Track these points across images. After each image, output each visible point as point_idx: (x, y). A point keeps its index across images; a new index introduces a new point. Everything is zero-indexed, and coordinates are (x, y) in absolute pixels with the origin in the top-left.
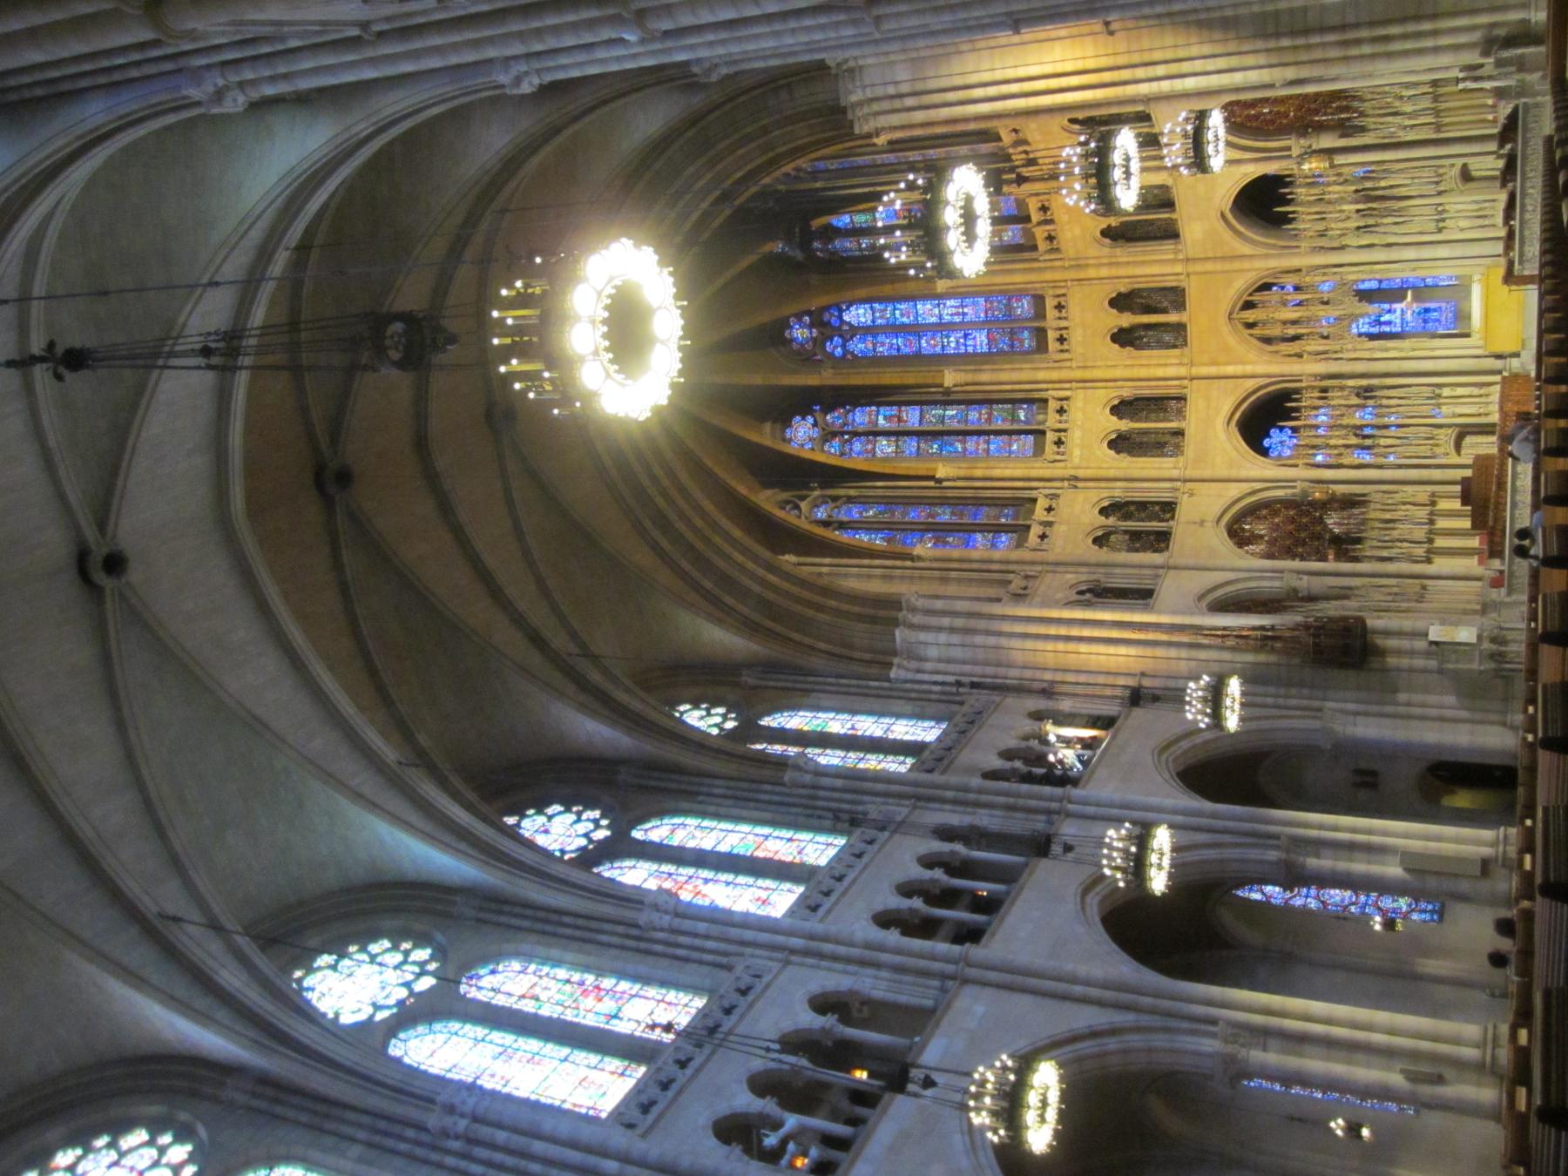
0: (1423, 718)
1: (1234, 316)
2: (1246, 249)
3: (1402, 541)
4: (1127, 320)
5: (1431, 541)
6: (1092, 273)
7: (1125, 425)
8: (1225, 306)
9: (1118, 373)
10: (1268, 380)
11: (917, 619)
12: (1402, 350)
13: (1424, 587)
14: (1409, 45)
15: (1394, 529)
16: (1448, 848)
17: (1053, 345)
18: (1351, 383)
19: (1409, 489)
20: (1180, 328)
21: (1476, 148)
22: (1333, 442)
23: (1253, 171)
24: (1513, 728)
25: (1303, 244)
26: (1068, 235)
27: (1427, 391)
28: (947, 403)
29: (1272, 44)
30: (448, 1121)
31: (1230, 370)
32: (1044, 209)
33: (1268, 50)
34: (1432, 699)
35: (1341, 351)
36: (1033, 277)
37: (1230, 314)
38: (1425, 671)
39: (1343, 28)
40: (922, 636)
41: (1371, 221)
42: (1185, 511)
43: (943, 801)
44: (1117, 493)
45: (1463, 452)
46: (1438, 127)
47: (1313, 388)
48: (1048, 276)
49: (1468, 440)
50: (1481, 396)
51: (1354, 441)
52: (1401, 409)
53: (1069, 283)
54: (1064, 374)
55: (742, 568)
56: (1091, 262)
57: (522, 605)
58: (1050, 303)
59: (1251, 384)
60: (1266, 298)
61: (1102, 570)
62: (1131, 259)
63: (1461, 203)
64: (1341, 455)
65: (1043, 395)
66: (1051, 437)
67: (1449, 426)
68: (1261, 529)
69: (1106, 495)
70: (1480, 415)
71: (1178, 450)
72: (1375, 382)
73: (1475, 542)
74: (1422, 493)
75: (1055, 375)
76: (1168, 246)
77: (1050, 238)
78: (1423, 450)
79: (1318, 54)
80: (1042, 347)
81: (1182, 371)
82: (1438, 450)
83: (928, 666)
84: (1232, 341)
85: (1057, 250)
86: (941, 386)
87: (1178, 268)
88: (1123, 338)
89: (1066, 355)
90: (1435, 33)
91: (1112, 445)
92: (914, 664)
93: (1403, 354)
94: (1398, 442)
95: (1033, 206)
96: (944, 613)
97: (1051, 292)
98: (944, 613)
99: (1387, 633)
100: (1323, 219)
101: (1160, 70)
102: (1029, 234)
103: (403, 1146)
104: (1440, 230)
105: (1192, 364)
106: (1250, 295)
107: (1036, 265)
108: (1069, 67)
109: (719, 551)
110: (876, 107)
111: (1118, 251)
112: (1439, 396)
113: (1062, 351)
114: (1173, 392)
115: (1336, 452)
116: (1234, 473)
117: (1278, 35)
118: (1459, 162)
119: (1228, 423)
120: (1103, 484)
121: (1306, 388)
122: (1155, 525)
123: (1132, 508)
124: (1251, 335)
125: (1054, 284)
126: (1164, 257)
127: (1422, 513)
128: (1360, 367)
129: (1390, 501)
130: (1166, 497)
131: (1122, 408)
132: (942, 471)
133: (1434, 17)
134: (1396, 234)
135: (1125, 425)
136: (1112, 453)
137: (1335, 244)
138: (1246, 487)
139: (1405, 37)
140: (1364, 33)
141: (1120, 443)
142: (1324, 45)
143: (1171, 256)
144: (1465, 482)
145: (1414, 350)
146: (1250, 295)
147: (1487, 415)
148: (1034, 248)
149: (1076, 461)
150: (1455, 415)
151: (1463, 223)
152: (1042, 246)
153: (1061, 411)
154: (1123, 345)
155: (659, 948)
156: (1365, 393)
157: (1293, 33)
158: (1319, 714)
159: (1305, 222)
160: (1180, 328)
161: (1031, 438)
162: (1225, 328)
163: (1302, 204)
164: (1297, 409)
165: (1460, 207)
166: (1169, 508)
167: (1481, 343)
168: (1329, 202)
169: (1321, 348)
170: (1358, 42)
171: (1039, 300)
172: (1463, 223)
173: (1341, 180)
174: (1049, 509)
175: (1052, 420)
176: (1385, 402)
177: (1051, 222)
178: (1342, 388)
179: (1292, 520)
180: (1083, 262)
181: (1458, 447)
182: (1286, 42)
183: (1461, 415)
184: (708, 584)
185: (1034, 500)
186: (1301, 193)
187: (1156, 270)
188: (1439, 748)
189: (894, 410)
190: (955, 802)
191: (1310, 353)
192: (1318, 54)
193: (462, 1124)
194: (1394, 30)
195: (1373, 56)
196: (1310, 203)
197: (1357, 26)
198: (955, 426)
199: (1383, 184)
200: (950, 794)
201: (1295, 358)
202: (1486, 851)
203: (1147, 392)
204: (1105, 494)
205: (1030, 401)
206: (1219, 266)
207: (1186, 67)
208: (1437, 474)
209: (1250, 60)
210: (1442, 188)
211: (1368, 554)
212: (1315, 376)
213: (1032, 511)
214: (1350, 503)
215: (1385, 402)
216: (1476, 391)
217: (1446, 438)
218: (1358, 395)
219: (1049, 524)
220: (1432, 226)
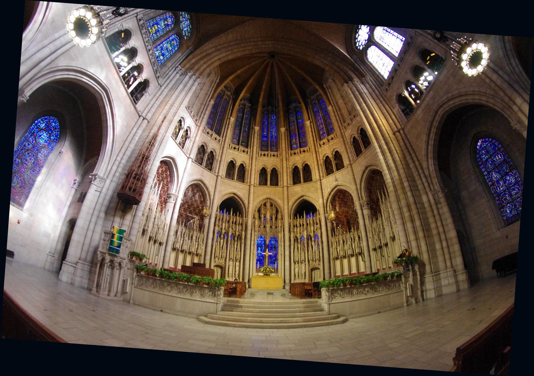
1: (268, 200)
2: (291, 204)
3: (183, 241)
5: (182, 251)
6: (285, 162)
8: (272, 197)
10: (247, 208)
12: (253, 250)
13: (160, 244)
15: (189, 239)
18: (243, 233)
19: (204, 248)
20: (266, 184)
21: (327, 271)
22: (224, 224)
23: (319, 203)
25: (292, 220)
26: (296, 157)
27: (238, 257)
29: (404, 179)
31: (252, 196)
33: (401, 180)
35: (255, 231)
36: (284, 149)
37: (270, 199)
41: (299, 241)
44: (217, 157)
45: (215, 268)
47: (243, 222)
48: (284, 152)
49: (219, 270)
50: (235, 275)
51: (223, 231)
52: (233, 248)
53: (281, 157)
56: (288, 163)
59: (246, 202)
60: (274, 209)
61: (193, 139)
62: (288, 173)
63: (304, 268)
64: (219, 227)
65: (249, 147)
67: (225, 263)
69: (217, 154)
70: (228, 274)
72: (243, 241)
76: (292, 183)
78: (217, 254)
79: (402, 196)
81: (252, 183)
82: (217, 259)
84: (261, 198)
85: (291, 155)
86: (255, 126)
87: (285, 184)
88: (263, 171)
89: (260, 155)
90: (417, 239)
91: (232, 162)
93: (252, 250)
94: (221, 246)
95: (305, 149)
97: (279, 153)
100: (300, 226)
101: (385, 147)
104: (295, 263)
105: (254, 186)
106: (275, 205)
107: (287, 150)
111: (291, 169)
112: (236, 261)
113: (261, 155)
115: (220, 225)
116: (217, 191)
118: (321, 267)
119: (234, 194)
120: (220, 154)
121: (243, 219)
123: (211, 161)
124: (262, 205)
125: (281, 154)
126: (289, 181)
127: (193, 250)
128: (249, 236)
129: (200, 240)
134: (294, 248)
136: (229, 161)
137: (292, 230)
138: (212, 193)
139: (414, 228)
140: (414, 212)
142: (406, 198)
143: (289, 183)
144: (204, 265)
145: (253, 254)
146: (275, 205)
147: (228, 276)
149: (229, 150)
150: (229, 266)
151: (297, 270)
152: (293, 152)
154: (261, 170)
156: (240, 237)
158: (105, 177)
159: (299, 221)
160: (266, 184)
162: (265, 197)
163: (306, 219)
164: (236, 215)
165: (303, 268)
167: (254, 276)
168: (307, 227)
169: (256, 225)
170: (410, 210)
172: (297, 270)
173: (315, 230)
174: (216, 139)
175: (242, 148)
176: (236, 243)
177: (301, 153)
178: (242, 230)
179: (198, 207)
180: (288, 160)
181: (217, 266)
182: (406, 184)
183: (229, 268)
186: (310, 219)
191: (254, 221)
192: (402, 196)
194: (418, 223)
195: (402, 218)
196: (306, 221)
199: (313, 243)
201: (253, 217)
206: (286, 195)
207: (388, 154)
208: (208, 257)
209: (395, 174)
210: (311, 262)
211: (180, 227)
212: (247, 222)
213: (216, 133)
214: (201, 227)
215: (236, 243)
216: (237, 273)
217: (221, 262)
218: (239, 235)
219: (211, 135)
220: (296, 259)
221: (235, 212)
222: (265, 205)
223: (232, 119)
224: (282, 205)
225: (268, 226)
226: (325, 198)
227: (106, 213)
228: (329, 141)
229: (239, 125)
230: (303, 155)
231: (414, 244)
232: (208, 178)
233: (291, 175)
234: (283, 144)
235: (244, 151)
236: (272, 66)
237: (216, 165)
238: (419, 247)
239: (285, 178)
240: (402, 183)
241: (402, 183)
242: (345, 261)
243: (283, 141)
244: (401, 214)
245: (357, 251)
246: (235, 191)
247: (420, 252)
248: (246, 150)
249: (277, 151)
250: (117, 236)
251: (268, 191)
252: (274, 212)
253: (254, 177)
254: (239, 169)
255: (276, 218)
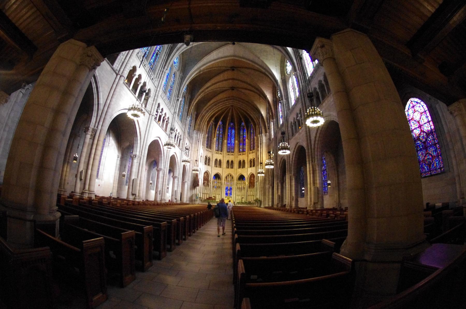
0: (187, 192)
2: (237, 176)
4: (230, 162)
6: (236, 159)
7: (218, 160)
8: (231, 173)
9: (224, 160)
11: (201, 134)
14: (261, 193)
16: (178, 195)
17: (228, 153)
21: (246, 199)
23: (246, 177)
24: (186, 202)
28: (222, 140)
29: (263, 180)
30: (165, 69)
31: (224, 173)
32: (244, 154)
34: (189, 193)
36: (236, 152)
38: (192, 193)
39: (264, 187)
40: (199, 135)
42: (208, 167)
43: (184, 136)
46: (248, 196)
48: (236, 154)
54: (225, 154)
55: (209, 114)
57: (212, 87)
58: (233, 154)
59: (222, 175)
63: (240, 197)
66: (218, 152)
68: (206, 175)
71: (215, 166)
73: (206, 198)
74: (209, 193)
75: (225, 153)
76: (238, 167)
77: (240, 154)
79: (261, 184)
80: (228, 152)
81: (224, 168)
83: (195, 135)
87: (236, 168)
88: (228, 161)
90: (262, 196)
92: (195, 133)
95: (244, 153)
96: (201, 138)
98: (201, 138)
99: (196, 189)
102: (241, 152)
103: (163, 63)
108: (263, 159)
109: (211, 111)
110: (261, 138)
114: (221, 166)
117: (264, 181)
122: (207, 164)
125: (235, 154)
127: (207, 193)
128: (223, 187)
130: (210, 165)
131: (220, 161)
132: (215, 139)
133: (264, 196)
135: (218, 160)
138: (211, 174)
139: (262, 193)
140: (263, 189)
141: (216, 160)
142: (262, 185)
148: (239, 152)
152: (240, 153)
153: (220, 154)
155: (175, 98)
156: (220, 187)
157: (264, 182)
159: (239, 182)
160: (228, 168)
161: (217, 150)
162: (228, 173)
166: (209, 165)
170: (262, 188)
171: (233, 152)
175: (220, 152)
181: (213, 196)
182: (263, 181)
184: (207, 109)
185: (211, 149)
187: (236, 166)
188: (184, 194)
189: (222, 134)
190: (184, 137)
192: (261, 184)
193: (165, 71)
194: (263, 192)
197: (264, 188)
198: (219, 141)
200: (185, 137)
202: (178, 199)
203: (222, 163)
204: (211, 158)
205: (222, 150)
208: (211, 194)
213: (209, 149)
217: (215, 195)
219: (208, 151)
221: (218, 179)
222: (228, 175)
223: (215, 139)
224: (234, 176)
225: (229, 183)
226: (248, 175)
227: (190, 189)
228: (252, 153)
229: (218, 140)
230: (243, 156)
231: (261, 197)
232: (209, 168)
233: (238, 164)
234: (236, 150)
235: (220, 154)
236: (232, 110)
237: (211, 162)
238: (262, 197)
239: (236, 165)
240: (262, 181)
241: (262, 181)
242: (251, 197)
243: (236, 148)
244: (260, 189)
245: (253, 195)
246: (218, 171)
247: (262, 199)
248: (221, 153)
249: (233, 153)
250: (197, 195)
251: (230, 171)
252: (231, 178)
253: (224, 164)
254: (219, 162)
255: (232, 181)
